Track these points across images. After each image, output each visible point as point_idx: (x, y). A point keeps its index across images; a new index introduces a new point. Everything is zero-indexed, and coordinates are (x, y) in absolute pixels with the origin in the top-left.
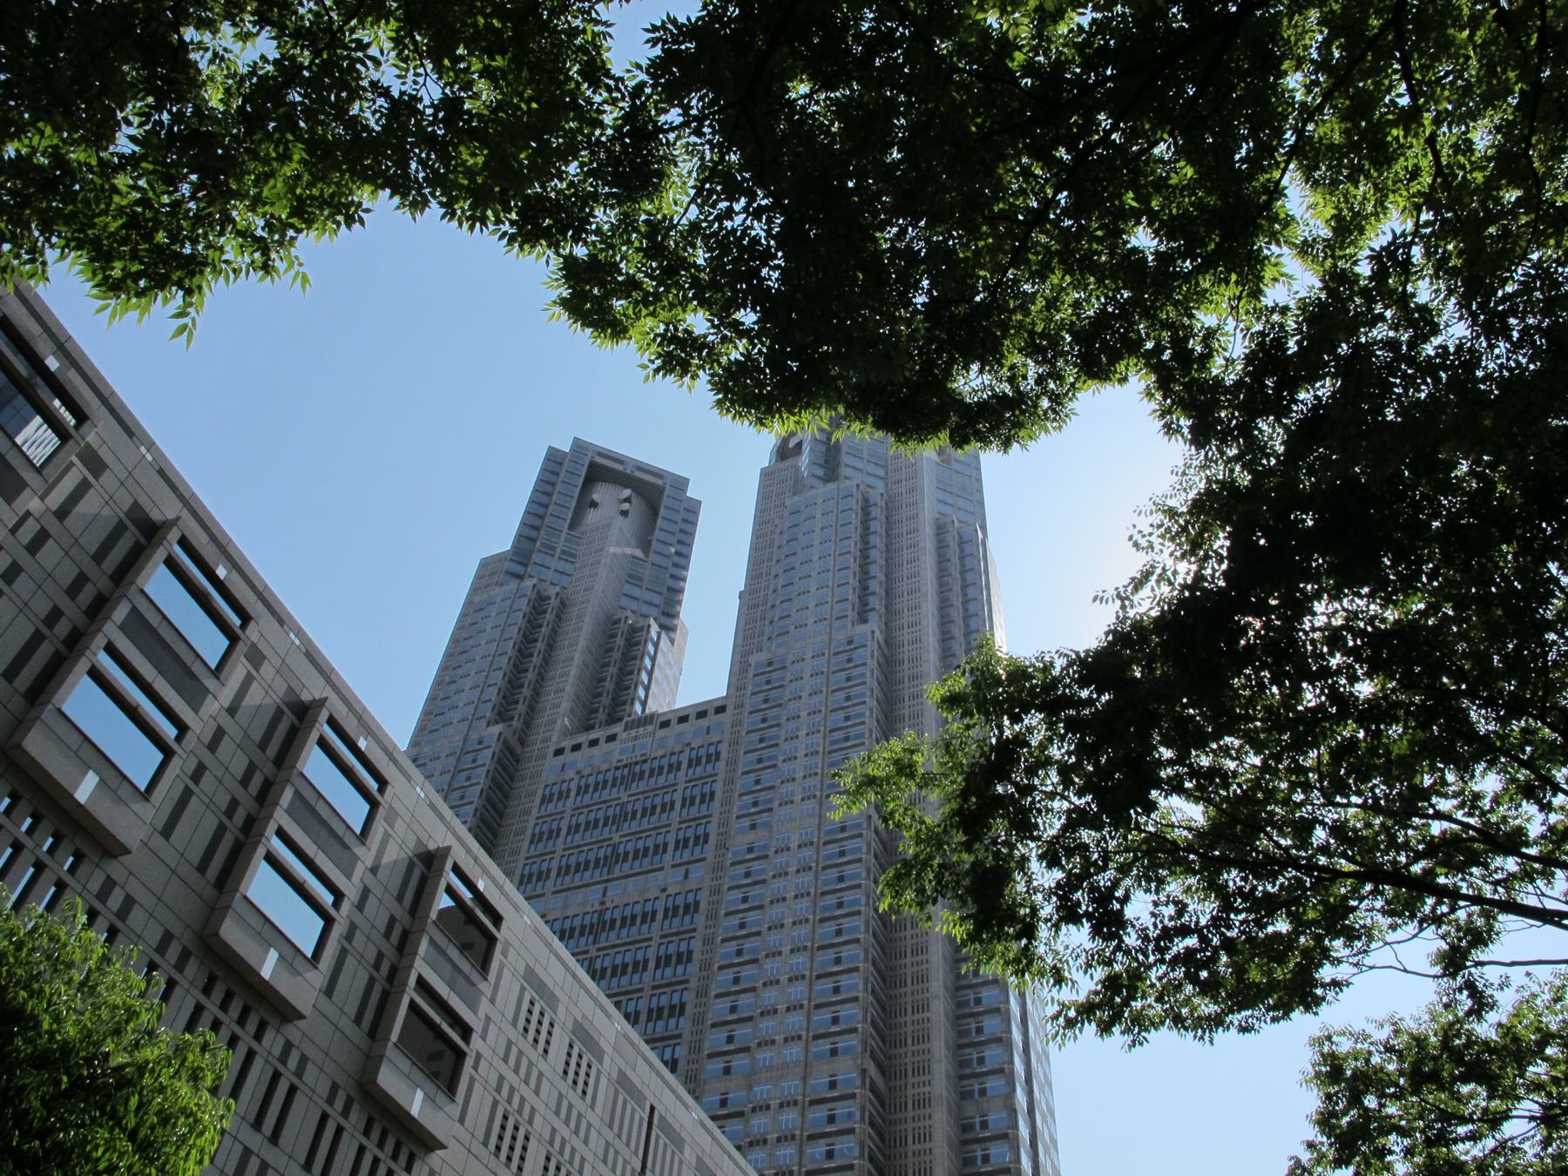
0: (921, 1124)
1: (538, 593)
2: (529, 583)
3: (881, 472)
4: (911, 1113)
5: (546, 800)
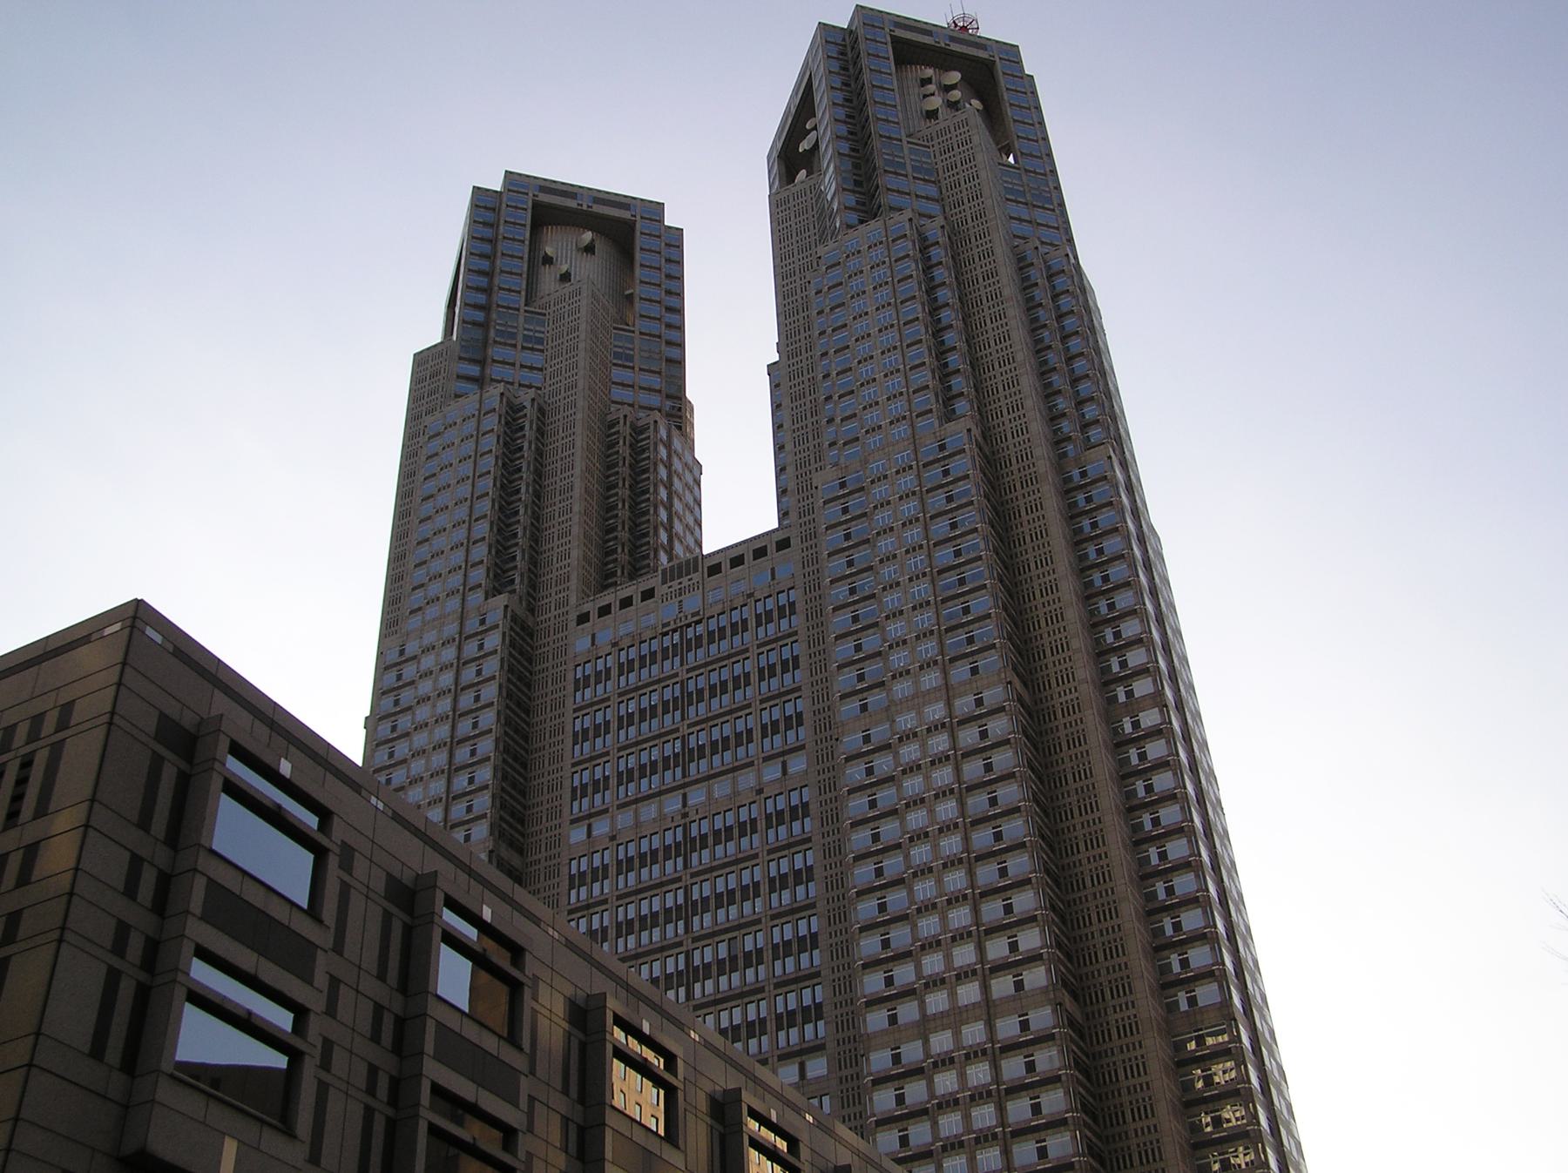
0: (1133, 1054)
1: (509, 402)
2: (494, 392)
3: (932, 191)
5: (582, 684)
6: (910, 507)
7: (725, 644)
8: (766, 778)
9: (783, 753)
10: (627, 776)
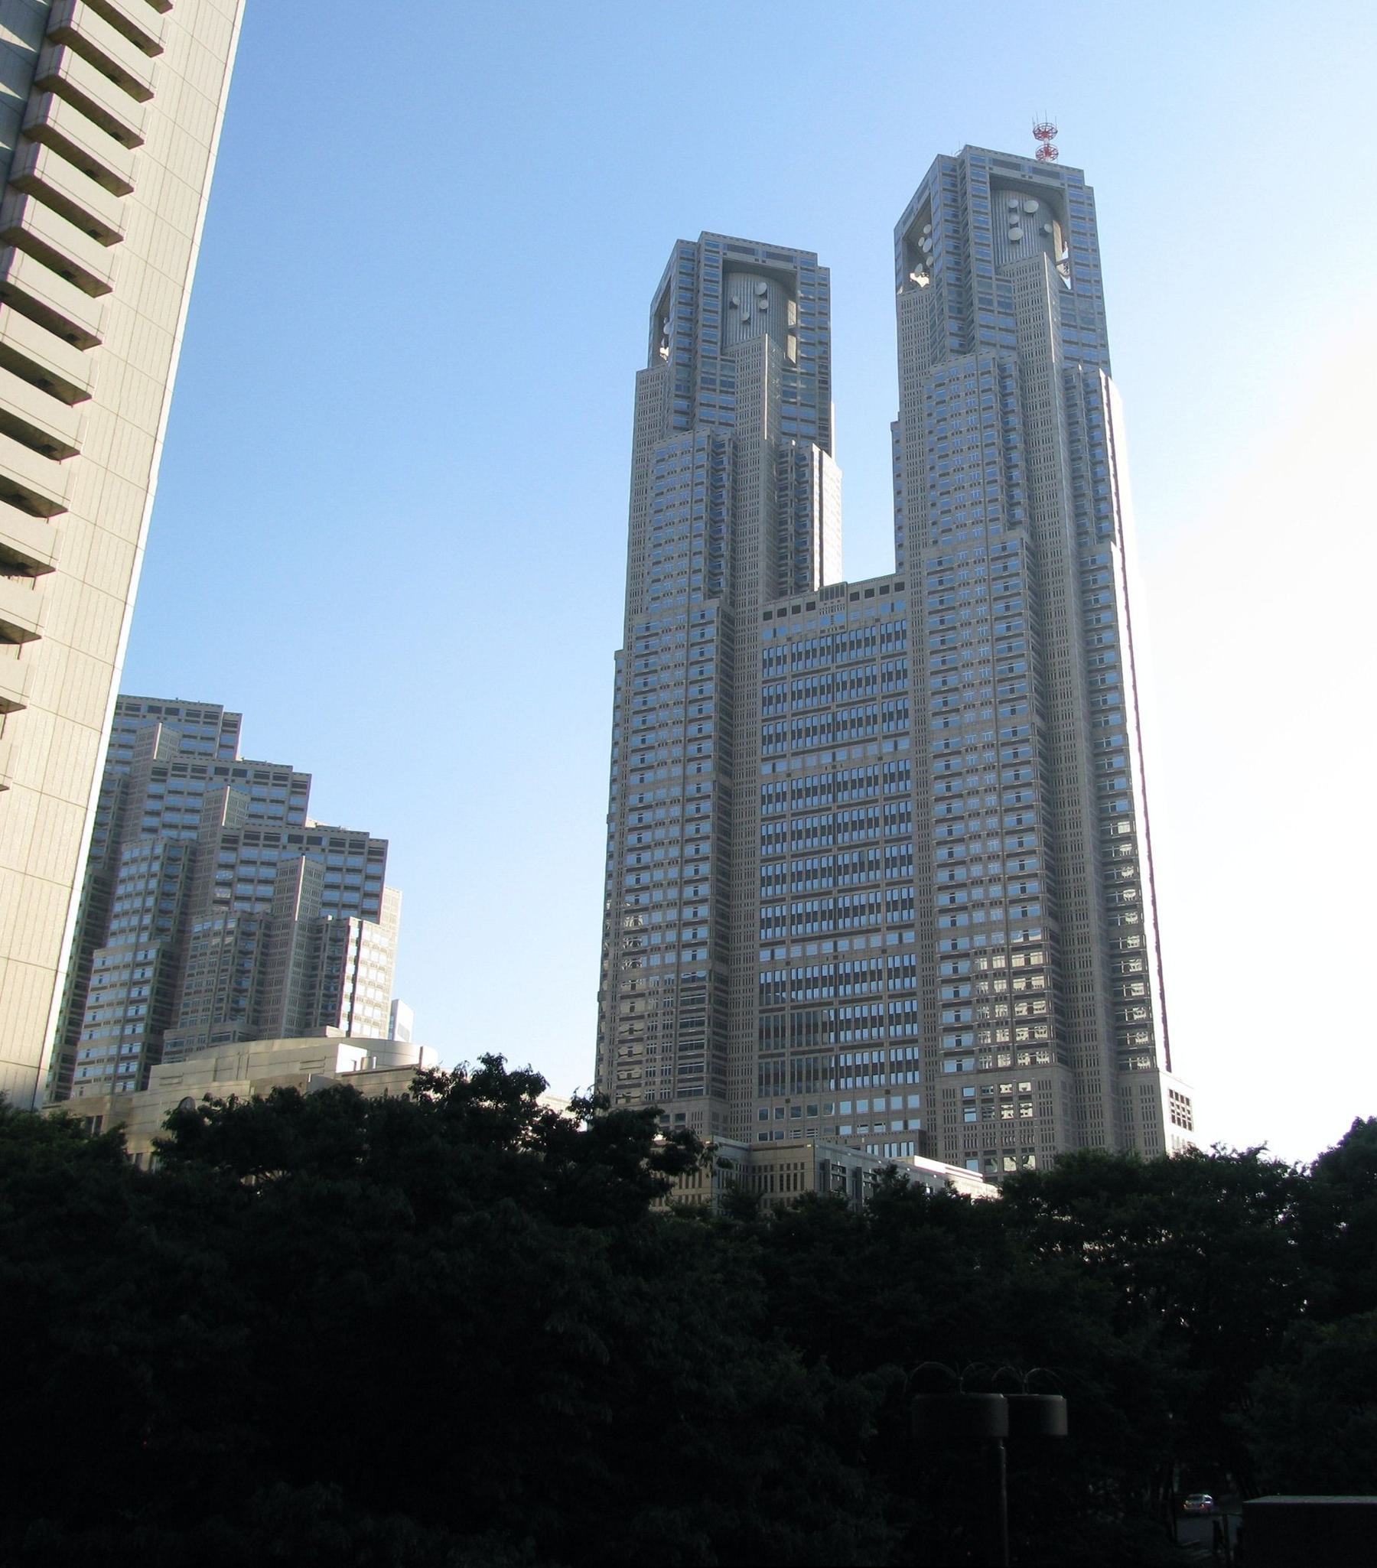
2: (703, 432)
4: (1077, 946)
5: (767, 663)
7: (860, 652)
8: (885, 750)
9: (896, 735)
10: (797, 734)
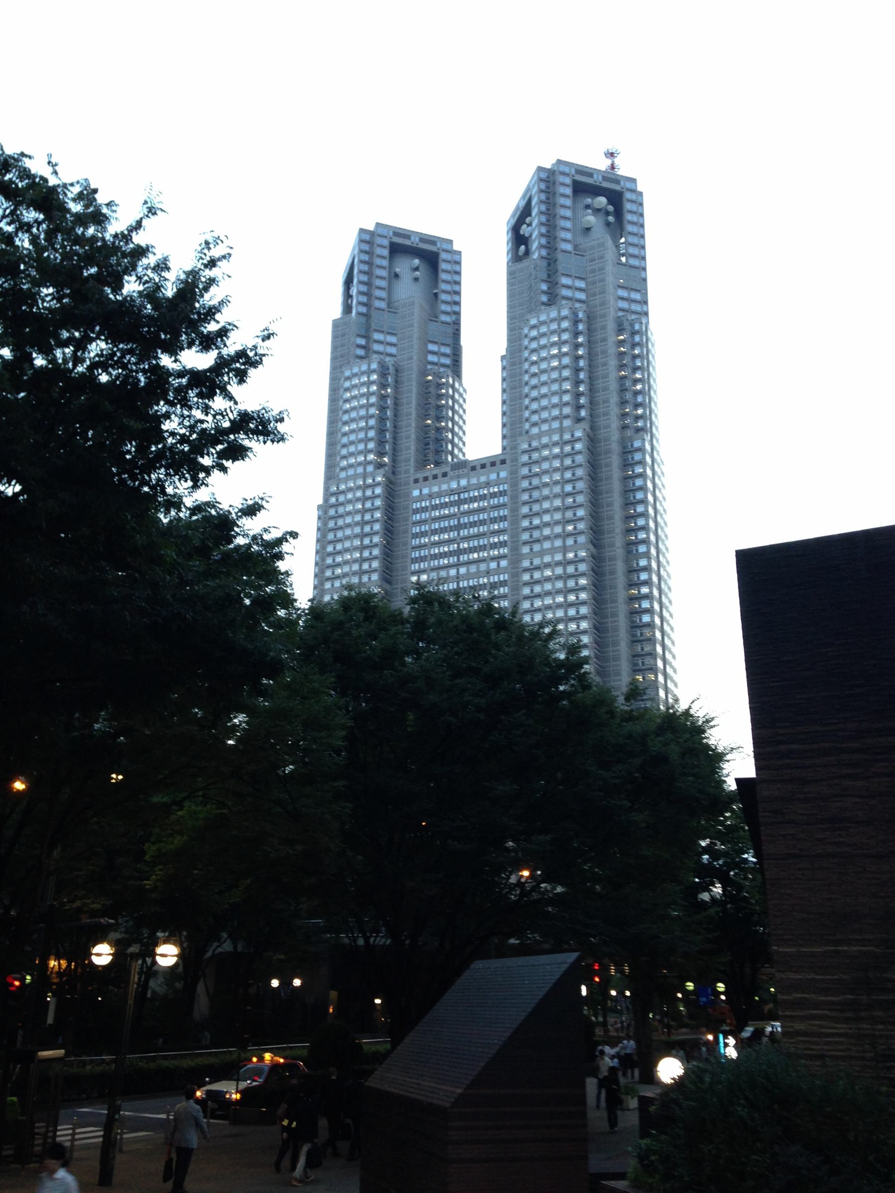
1: (383, 366)
3: (582, 284)
6: (557, 464)
